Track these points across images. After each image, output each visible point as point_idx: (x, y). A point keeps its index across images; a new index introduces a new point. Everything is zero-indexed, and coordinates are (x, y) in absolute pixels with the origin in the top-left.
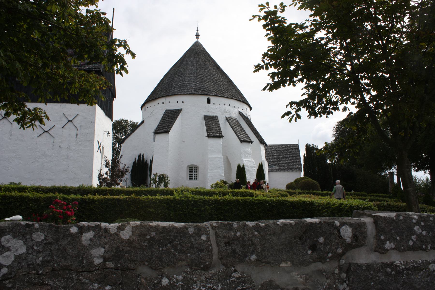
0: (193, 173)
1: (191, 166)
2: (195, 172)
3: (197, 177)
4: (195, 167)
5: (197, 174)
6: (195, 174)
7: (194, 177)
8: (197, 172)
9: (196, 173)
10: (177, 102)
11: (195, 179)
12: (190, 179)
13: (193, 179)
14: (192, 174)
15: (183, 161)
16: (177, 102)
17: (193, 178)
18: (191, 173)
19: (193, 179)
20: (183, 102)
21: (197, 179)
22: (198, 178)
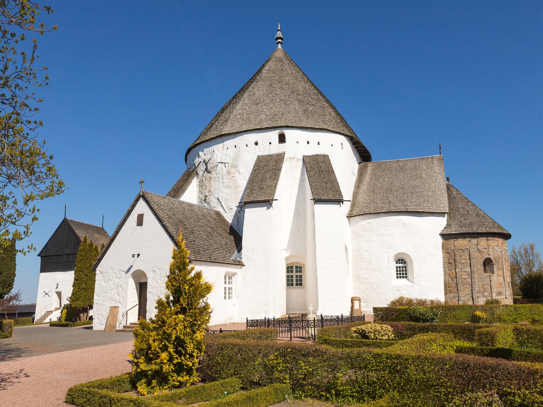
0: (294, 274)
3: (301, 280)
5: (301, 276)
6: (297, 276)
7: (297, 280)
8: (301, 271)
9: (299, 274)
11: (297, 285)
13: (294, 284)
14: (292, 276)
17: (294, 282)
18: (290, 274)
19: (294, 284)
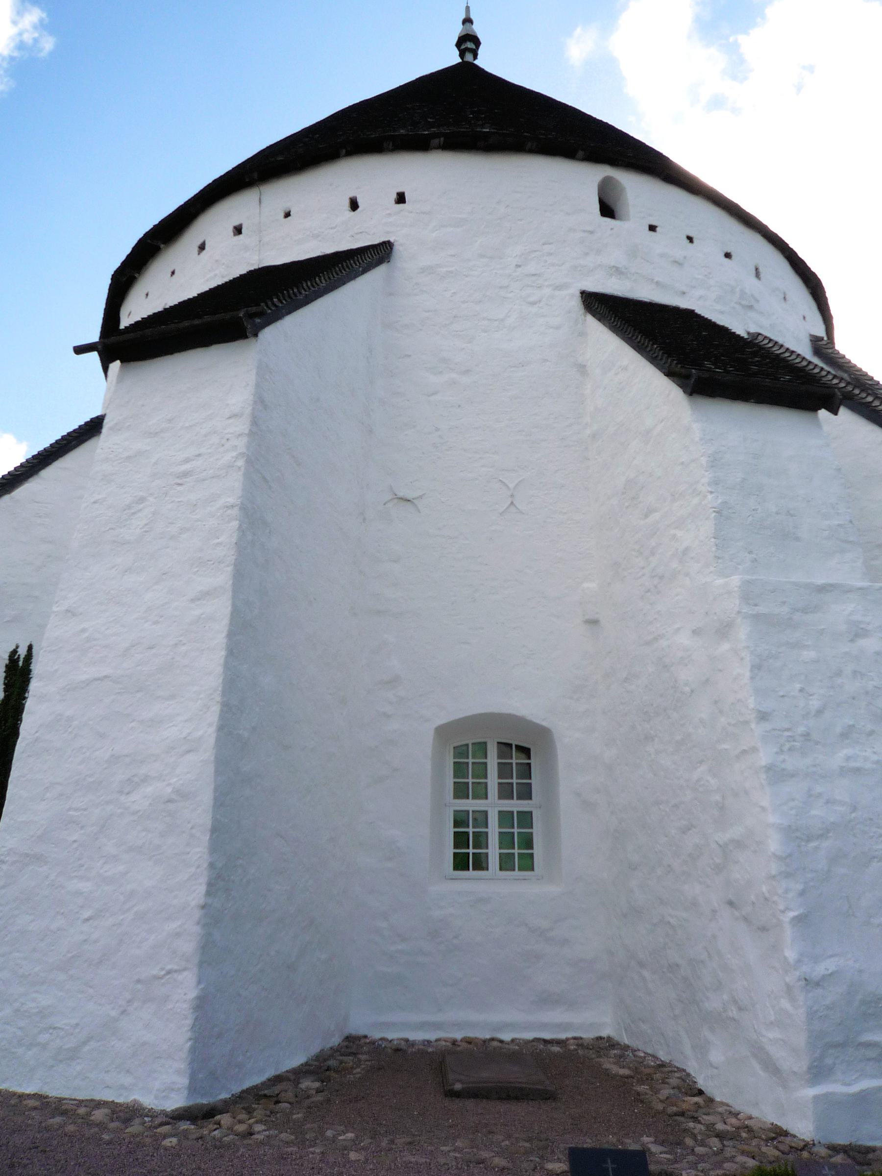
1: (470, 740)
2: (505, 792)
4: (505, 747)
5: (526, 818)
6: (505, 817)
7: (506, 840)
8: (526, 793)
9: (515, 805)
10: (354, 205)
11: (506, 864)
12: (461, 863)
15: (394, 681)
16: (354, 205)
19: (494, 860)
20: (401, 198)
21: (528, 863)
22: (538, 851)
